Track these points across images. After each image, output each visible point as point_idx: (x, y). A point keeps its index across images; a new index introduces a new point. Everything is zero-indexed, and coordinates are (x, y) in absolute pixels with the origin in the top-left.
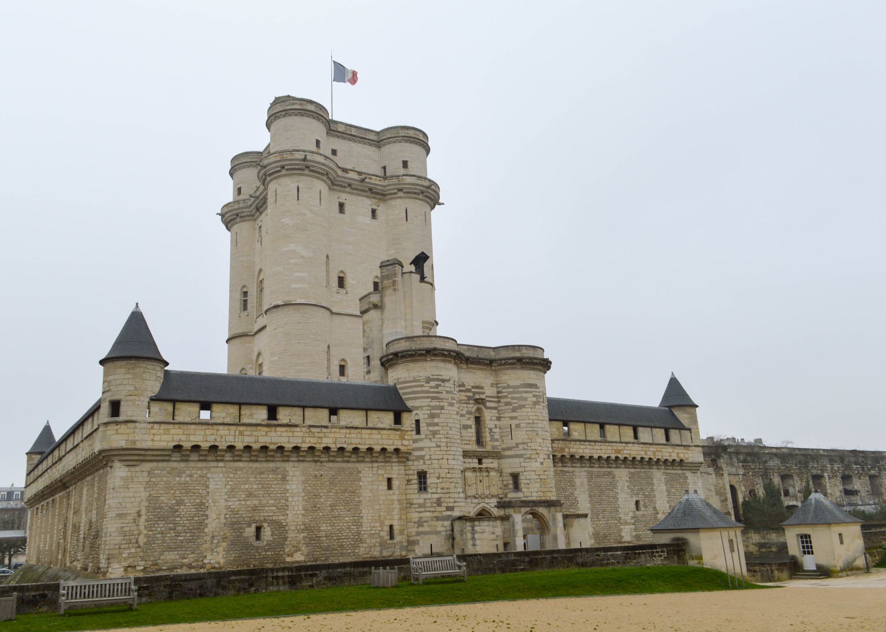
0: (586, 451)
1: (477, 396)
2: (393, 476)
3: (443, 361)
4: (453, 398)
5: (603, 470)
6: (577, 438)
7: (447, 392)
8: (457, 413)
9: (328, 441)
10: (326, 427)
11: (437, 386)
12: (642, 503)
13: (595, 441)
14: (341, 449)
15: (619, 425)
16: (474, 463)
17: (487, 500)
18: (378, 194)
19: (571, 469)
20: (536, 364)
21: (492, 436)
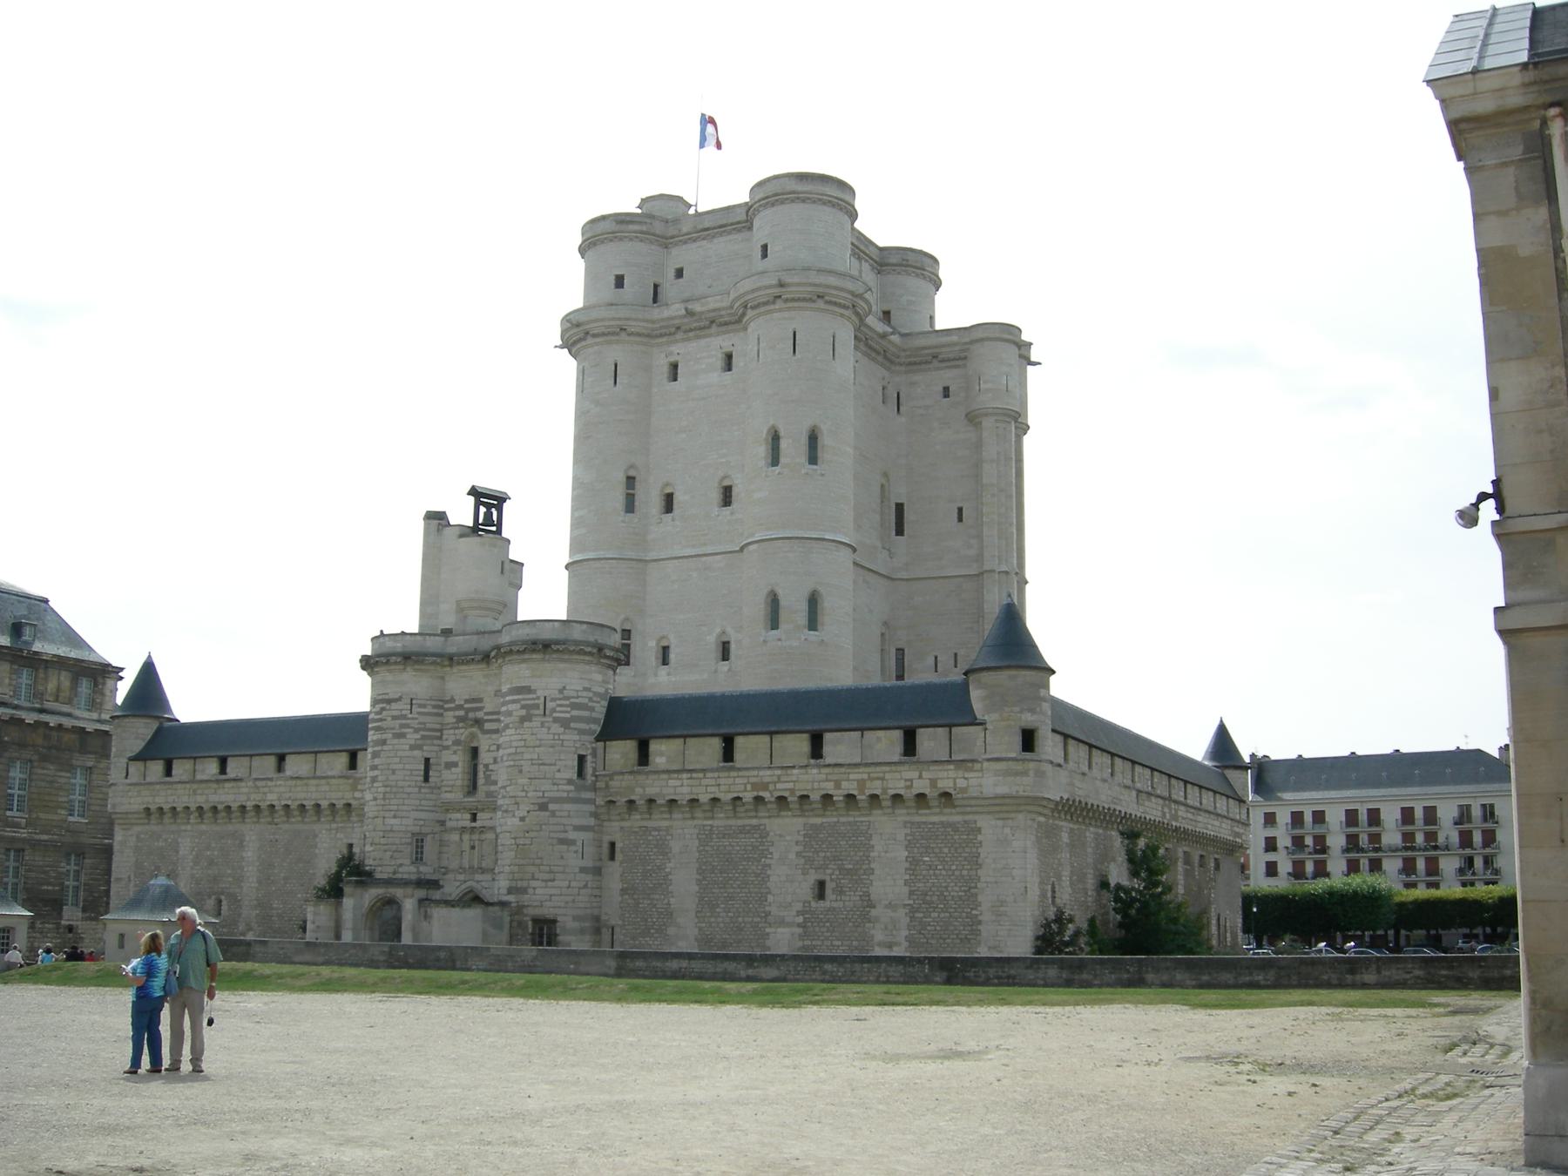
0: (679, 790)
1: (471, 715)
2: (354, 841)
3: (390, 671)
4: (402, 726)
5: (740, 822)
6: (662, 767)
7: (395, 718)
8: (413, 748)
9: (272, 798)
10: (271, 779)
11: (383, 709)
12: (829, 886)
13: (703, 771)
14: (287, 806)
15: (771, 734)
16: (463, 819)
17: (478, 877)
18: (726, 324)
19: (665, 824)
20: (524, 652)
21: (487, 778)
